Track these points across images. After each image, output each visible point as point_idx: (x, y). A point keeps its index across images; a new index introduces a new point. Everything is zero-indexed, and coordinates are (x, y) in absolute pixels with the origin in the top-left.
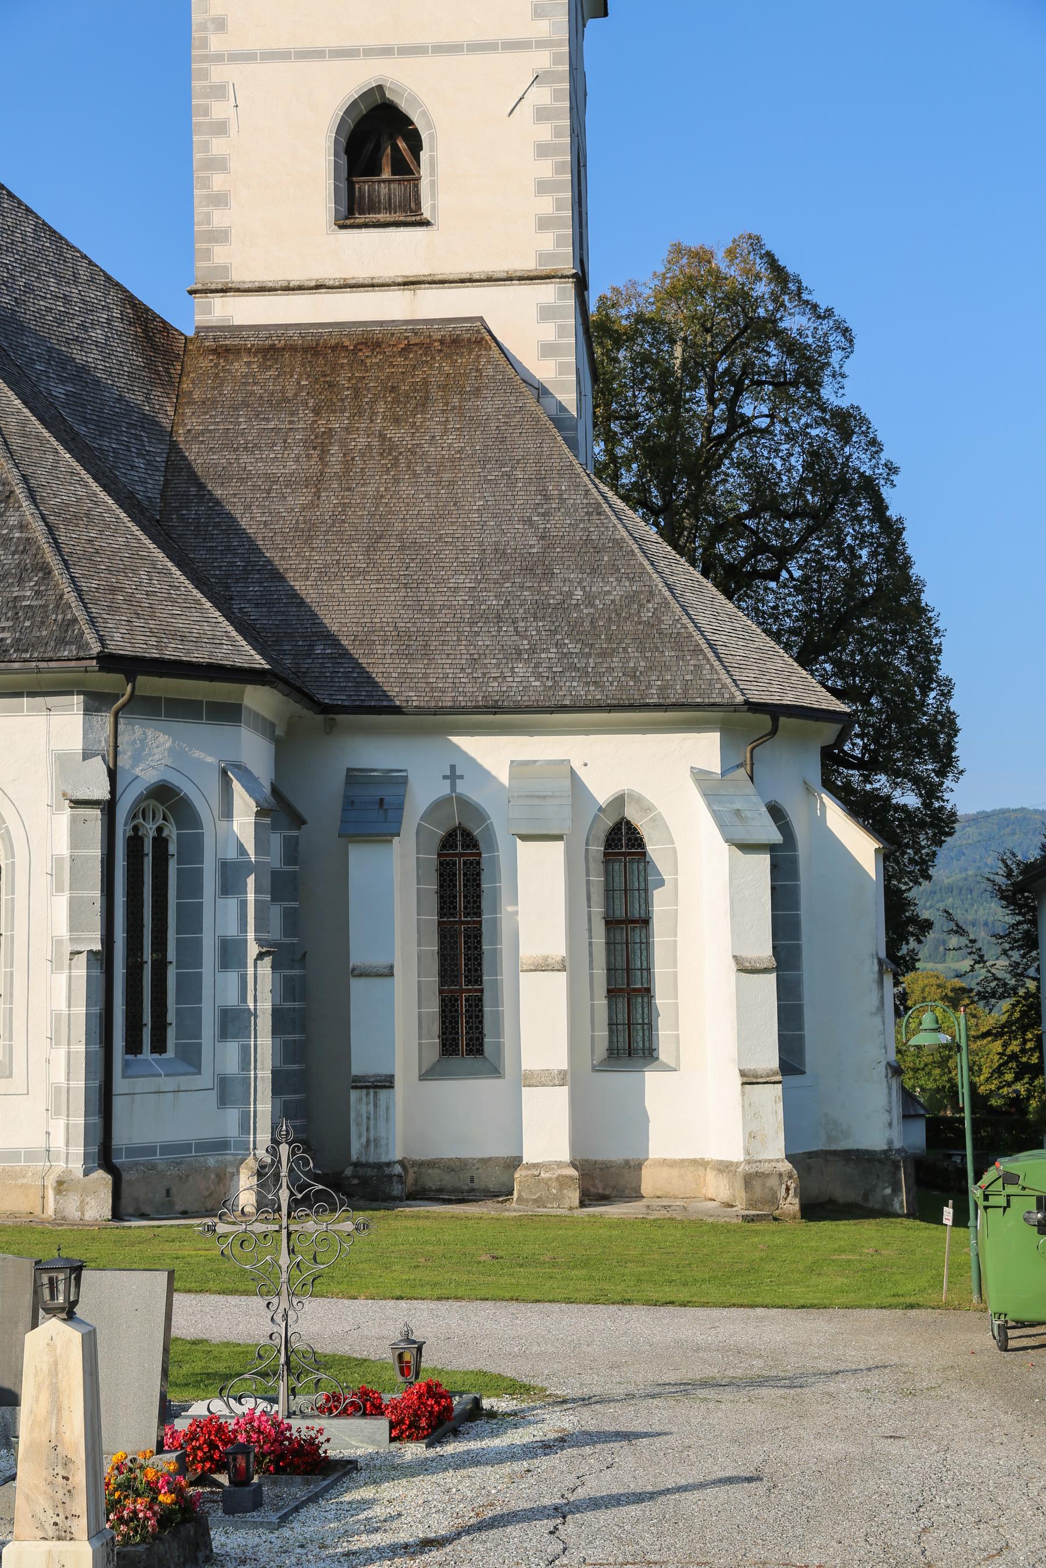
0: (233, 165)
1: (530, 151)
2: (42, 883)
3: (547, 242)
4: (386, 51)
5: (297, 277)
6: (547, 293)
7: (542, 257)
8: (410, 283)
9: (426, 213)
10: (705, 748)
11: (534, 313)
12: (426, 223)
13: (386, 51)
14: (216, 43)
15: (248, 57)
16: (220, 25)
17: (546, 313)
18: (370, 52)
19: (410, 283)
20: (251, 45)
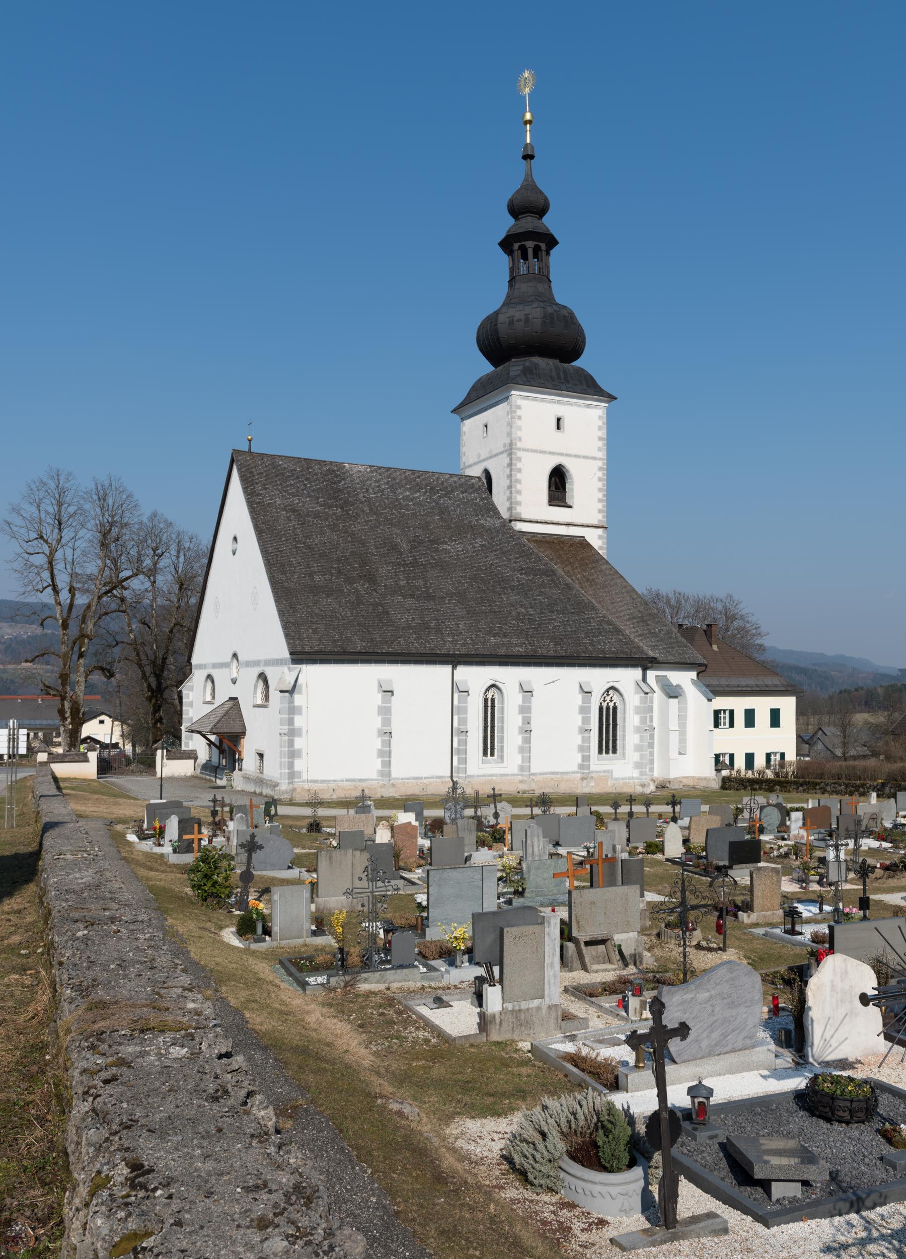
0: (523, 482)
1: (597, 490)
2: (632, 712)
3: (600, 516)
4: (562, 454)
5: (539, 519)
6: (600, 531)
7: (599, 521)
8: (568, 525)
9: (568, 501)
10: (693, 675)
11: (597, 537)
12: (571, 507)
13: (562, 454)
14: (519, 445)
15: (527, 450)
16: (520, 439)
17: (600, 537)
18: (559, 454)
19: (568, 525)
20: (527, 447)
